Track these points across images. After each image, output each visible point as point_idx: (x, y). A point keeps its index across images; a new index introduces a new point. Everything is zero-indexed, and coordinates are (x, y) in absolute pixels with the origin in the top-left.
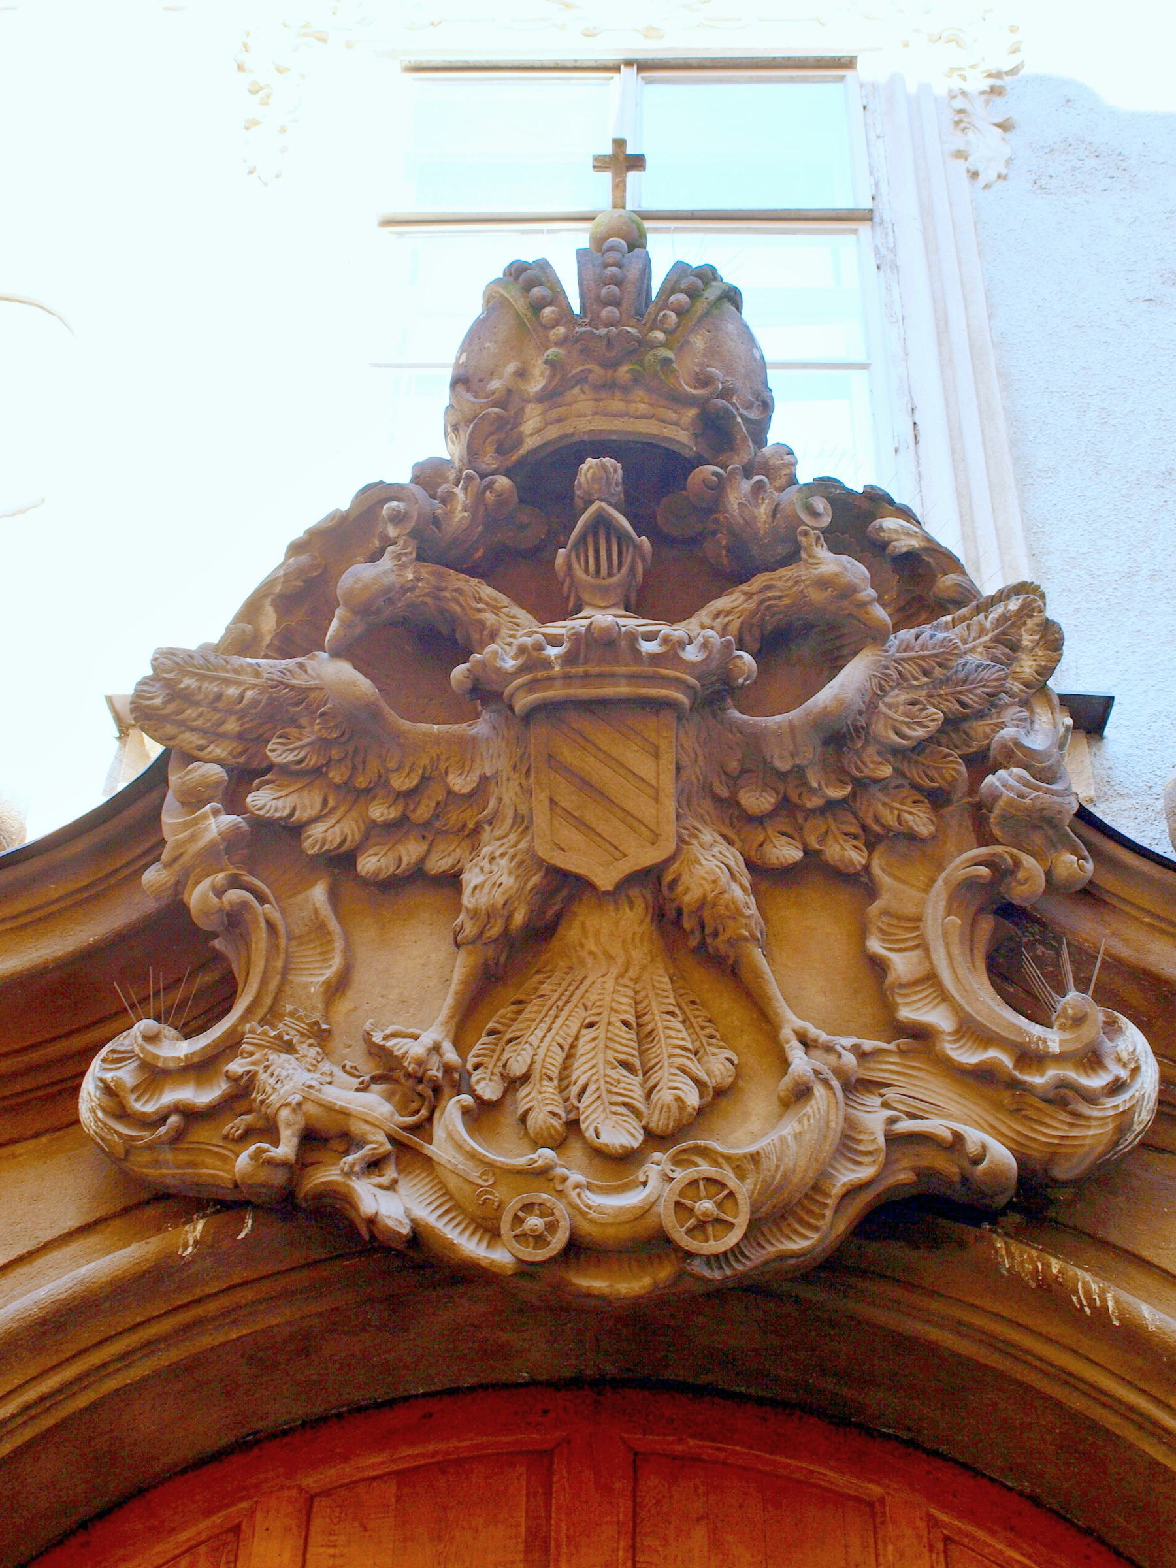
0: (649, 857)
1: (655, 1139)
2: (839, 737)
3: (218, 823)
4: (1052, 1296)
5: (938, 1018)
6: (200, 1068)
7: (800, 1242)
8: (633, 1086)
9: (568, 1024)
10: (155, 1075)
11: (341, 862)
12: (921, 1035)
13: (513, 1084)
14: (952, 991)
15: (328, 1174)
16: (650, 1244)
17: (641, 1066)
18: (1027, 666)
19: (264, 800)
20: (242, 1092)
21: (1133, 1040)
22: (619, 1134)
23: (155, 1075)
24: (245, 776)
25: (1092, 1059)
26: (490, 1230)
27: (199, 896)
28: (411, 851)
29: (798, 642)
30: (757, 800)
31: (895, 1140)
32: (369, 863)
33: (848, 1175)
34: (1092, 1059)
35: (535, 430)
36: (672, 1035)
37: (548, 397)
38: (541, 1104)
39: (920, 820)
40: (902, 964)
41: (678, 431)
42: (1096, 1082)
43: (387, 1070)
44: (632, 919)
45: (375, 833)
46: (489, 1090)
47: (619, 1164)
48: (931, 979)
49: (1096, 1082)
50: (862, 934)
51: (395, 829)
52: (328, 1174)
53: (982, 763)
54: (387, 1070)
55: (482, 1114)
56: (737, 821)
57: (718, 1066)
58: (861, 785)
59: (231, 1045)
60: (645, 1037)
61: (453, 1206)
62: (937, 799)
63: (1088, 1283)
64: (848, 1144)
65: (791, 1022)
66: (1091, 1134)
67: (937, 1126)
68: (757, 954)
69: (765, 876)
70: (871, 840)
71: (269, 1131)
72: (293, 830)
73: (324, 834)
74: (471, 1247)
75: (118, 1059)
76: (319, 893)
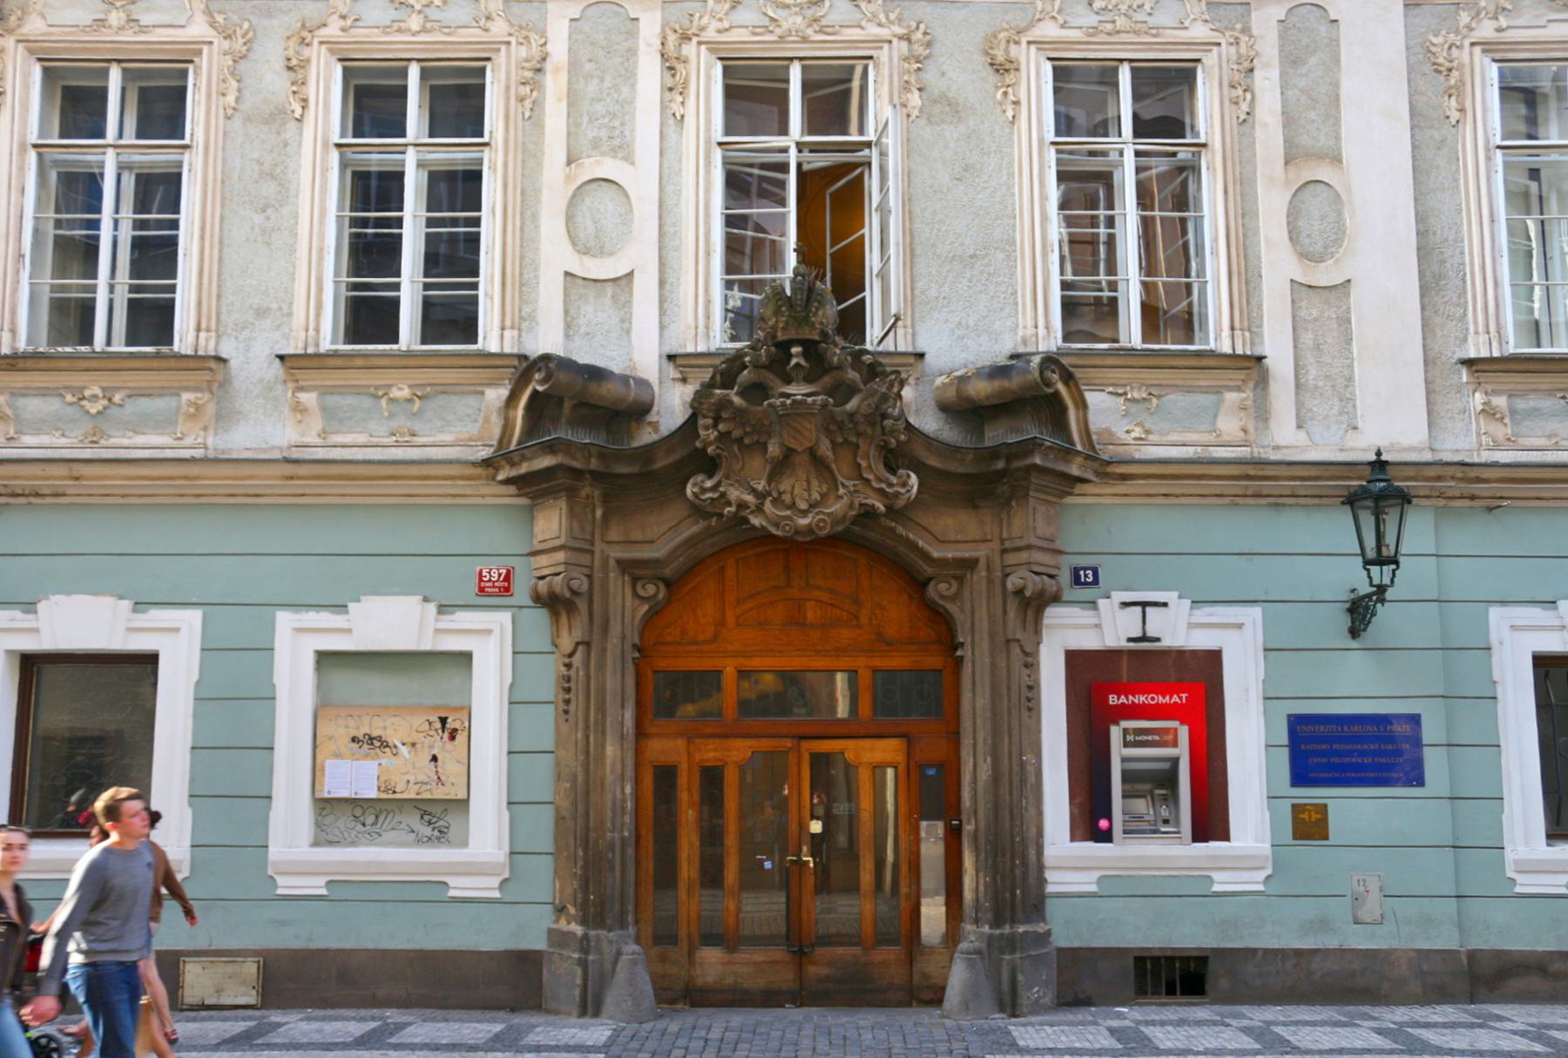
0: (809, 445)
1: (811, 506)
2: (851, 415)
3: (713, 435)
4: (893, 530)
5: (871, 477)
6: (714, 488)
7: (840, 528)
8: (806, 495)
9: (792, 481)
10: (704, 490)
11: (740, 440)
12: (868, 481)
13: (780, 493)
14: (873, 467)
15: (745, 513)
16: (810, 530)
17: (808, 490)
18: (895, 390)
19: (721, 427)
20: (723, 495)
21: (914, 479)
22: (804, 506)
23: (704, 490)
24: (717, 420)
25: (904, 485)
26: (777, 525)
27: (710, 450)
28: (755, 438)
29: (842, 391)
30: (833, 427)
31: (861, 505)
32: (747, 441)
33: (853, 513)
34: (904, 485)
35: (781, 336)
36: (815, 483)
37: (783, 329)
38: (787, 498)
39: (869, 431)
40: (864, 464)
41: (817, 338)
42: (903, 491)
43: (753, 491)
44: (805, 456)
45: (746, 434)
46: (775, 495)
47: (804, 513)
48: (870, 466)
49: (903, 491)
50: (855, 456)
51: (753, 432)
52: (745, 513)
53: (884, 416)
54: (753, 491)
55: (775, 502)
56: (828, 431)
57: (824, 488)
58: (856, 424)
59: (718, 484)
60: (809, 483)
61: (769, 521)
62: (873, 424)
63: (900, 530)
64: (851, 506)
65: (840, 479)
66: (901, 502)
67: (870, 501)
68: (833, 466)
69: (835, 446)
70: (859, 435)
71: (729, 504)
72: (729, 433)
73: (736, 433)
74: (773, 530)
75: (695, 485)
76: (736, 448)
